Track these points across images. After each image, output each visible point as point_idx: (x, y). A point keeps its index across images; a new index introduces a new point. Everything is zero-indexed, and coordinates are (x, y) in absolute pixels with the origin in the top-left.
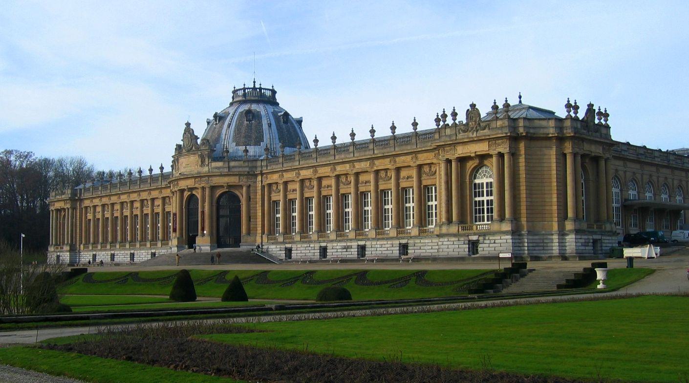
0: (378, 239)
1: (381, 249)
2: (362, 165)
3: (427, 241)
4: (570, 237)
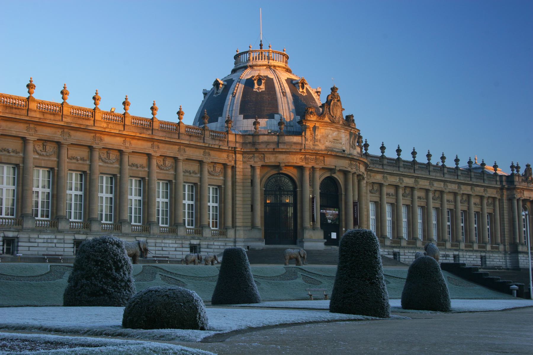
0: (467, 251)
1: (470, 259)
2: (453, 187)
3: (496, 255)
4: (521, 261)
